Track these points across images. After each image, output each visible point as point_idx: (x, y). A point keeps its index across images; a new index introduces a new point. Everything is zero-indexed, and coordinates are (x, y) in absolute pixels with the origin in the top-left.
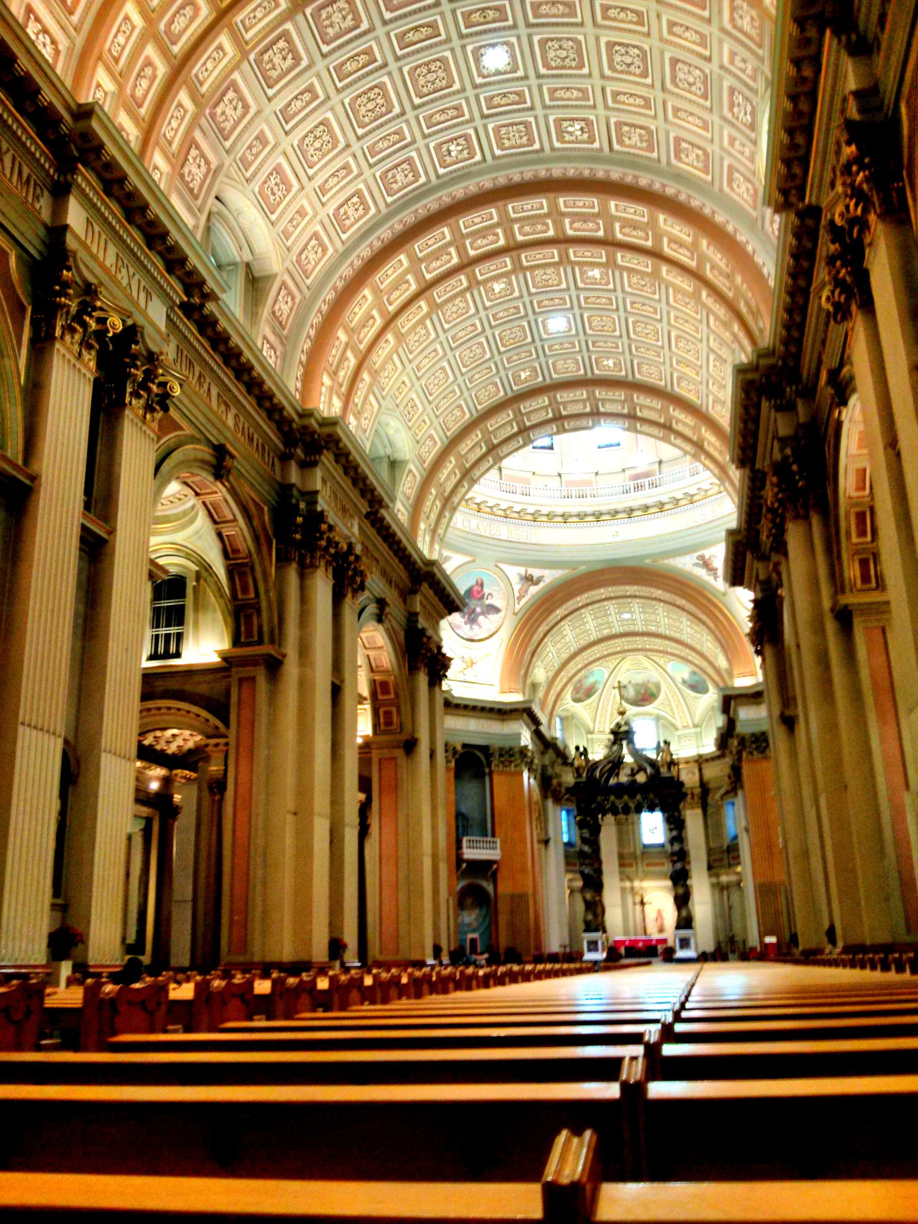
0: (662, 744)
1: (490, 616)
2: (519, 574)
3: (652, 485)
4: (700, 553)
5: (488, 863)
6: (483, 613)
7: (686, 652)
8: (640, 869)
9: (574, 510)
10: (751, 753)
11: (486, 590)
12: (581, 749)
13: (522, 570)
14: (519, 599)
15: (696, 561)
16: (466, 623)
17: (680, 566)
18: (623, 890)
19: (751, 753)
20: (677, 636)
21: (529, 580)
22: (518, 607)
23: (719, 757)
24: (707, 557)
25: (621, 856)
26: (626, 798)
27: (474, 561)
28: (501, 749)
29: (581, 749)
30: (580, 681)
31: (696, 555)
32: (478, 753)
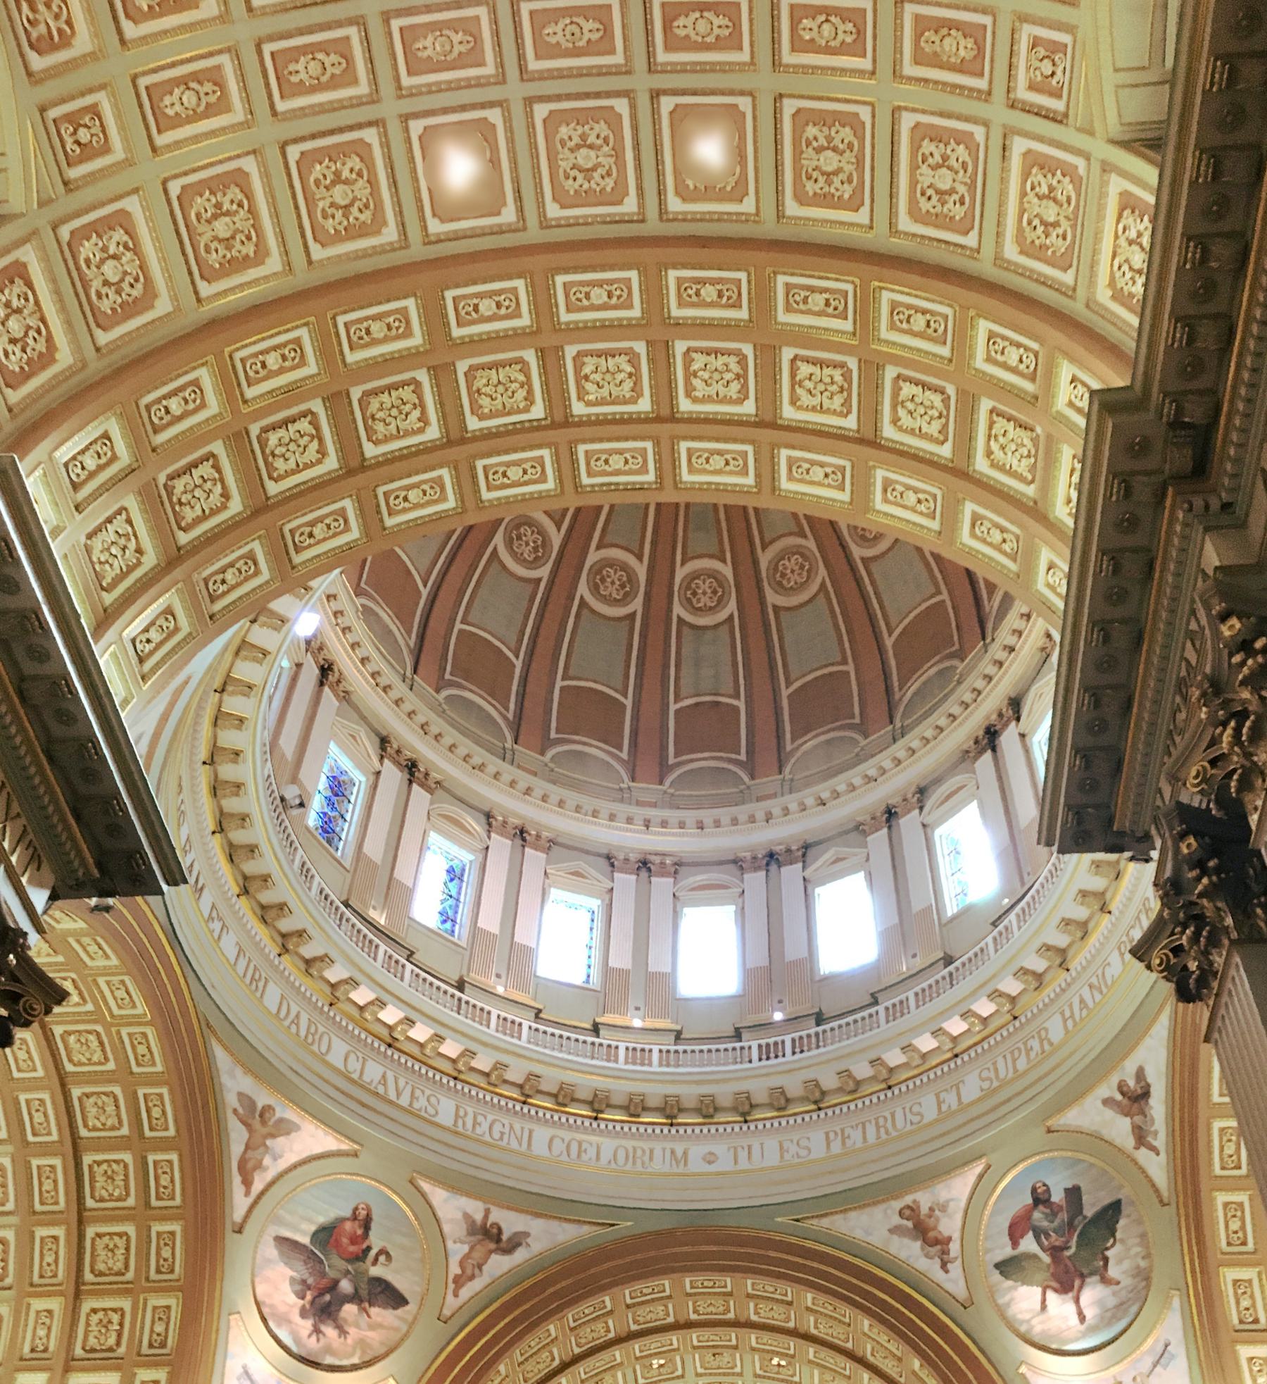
1: (374, 1311)
2: (466, 1216)
3: (799, 1046)
4: (908, 1200)
6: (355, 1298)
9: (621, 1089)
11: (376, 1240)
13: (476, 1209)
14: (459, 1282)
15: (896, 1220)
16: (303, 1313)
17: (859, 1234)
22: (452, 1303)
24: (924, 1210)
27: (356, 1155)
31: (897, 1205)
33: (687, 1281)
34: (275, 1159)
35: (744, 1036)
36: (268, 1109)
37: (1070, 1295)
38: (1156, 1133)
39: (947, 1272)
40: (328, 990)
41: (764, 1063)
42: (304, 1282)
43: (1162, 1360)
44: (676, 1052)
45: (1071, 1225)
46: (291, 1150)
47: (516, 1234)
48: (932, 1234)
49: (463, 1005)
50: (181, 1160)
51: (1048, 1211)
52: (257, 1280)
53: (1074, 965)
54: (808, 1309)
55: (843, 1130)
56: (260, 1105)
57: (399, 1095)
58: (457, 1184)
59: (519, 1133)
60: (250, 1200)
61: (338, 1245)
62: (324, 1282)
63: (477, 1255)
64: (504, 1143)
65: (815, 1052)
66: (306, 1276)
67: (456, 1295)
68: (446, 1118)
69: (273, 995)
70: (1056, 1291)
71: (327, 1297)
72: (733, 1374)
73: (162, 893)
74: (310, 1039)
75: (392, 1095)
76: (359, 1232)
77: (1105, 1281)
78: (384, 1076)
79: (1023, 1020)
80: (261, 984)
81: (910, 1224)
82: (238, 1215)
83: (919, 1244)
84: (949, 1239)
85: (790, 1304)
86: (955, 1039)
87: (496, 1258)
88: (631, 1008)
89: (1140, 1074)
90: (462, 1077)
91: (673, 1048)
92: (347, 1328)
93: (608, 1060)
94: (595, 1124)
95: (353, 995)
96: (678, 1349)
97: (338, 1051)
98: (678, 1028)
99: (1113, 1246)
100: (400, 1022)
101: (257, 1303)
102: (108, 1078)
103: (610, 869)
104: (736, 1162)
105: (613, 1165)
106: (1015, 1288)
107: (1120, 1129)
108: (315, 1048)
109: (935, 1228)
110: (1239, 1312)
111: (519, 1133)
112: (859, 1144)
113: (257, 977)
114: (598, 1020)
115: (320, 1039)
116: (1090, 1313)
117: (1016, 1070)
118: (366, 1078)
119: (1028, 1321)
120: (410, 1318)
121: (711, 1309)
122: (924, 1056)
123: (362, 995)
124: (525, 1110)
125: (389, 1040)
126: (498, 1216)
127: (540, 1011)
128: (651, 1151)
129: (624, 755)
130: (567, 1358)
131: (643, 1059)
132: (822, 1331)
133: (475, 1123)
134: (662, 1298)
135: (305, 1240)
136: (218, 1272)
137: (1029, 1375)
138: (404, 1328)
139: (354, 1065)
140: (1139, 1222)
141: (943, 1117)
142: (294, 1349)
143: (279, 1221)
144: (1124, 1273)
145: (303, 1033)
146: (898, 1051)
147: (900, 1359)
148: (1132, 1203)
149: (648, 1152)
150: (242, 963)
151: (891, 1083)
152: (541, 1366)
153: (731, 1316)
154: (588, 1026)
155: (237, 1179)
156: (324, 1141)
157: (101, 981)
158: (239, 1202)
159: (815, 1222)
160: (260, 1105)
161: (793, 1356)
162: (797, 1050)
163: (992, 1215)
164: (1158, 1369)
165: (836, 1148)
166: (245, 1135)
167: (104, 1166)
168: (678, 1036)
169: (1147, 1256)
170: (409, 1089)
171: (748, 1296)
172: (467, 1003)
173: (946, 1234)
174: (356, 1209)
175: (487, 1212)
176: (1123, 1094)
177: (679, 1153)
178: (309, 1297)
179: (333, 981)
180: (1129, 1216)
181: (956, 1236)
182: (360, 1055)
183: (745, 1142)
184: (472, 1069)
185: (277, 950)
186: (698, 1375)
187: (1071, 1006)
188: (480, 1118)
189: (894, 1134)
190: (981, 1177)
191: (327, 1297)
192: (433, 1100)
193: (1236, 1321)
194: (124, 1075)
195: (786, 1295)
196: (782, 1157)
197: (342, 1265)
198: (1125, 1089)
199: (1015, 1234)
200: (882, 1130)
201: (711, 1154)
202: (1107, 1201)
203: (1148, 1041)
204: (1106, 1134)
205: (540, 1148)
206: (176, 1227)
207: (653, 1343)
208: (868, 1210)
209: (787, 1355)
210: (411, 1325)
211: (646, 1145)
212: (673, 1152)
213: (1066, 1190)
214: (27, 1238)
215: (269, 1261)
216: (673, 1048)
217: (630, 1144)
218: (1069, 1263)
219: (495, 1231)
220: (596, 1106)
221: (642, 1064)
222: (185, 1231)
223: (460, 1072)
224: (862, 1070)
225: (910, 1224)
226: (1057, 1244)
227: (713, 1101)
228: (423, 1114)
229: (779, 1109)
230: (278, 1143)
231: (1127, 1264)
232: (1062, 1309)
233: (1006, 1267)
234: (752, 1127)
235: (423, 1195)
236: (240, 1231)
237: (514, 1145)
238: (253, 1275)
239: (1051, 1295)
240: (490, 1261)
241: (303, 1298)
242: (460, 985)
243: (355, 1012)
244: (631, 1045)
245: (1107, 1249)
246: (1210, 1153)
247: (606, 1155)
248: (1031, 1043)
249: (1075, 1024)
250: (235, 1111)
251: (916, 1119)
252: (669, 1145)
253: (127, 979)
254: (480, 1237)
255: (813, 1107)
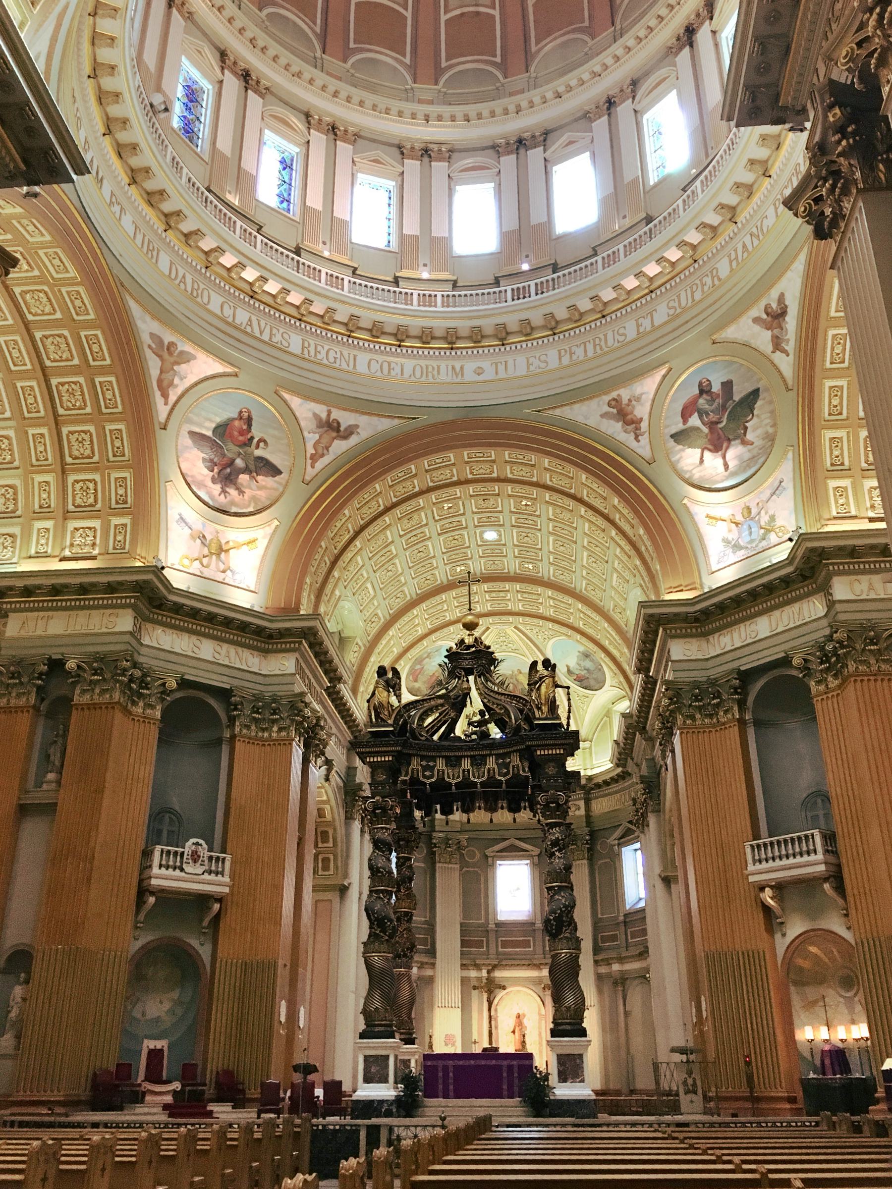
0: (540, 667)
1: (259, 478)
2: (315, 415)
4: (614, 394)
5: (203, 900)
6: (247, 470)
7: (577, 613)
8: (493, 950)
9: (415, 324)
10: (693, 718)
11: (256, 432)
12: (390, 675)
13: (321, 410)
14: (314, 458)
15: (606, 409)
16: (214, 480)
17: (580, 419)
18: (464, 981)
19: (693, 718)
20: (564, 579)
21: (331, 427)
22: (310, 472)
23: (614, 780)
24: (625, 401)
25: (465, 930)
26: (466, 764)
27: (236, 375)
28: (257, 698)
29: (390, 675)
30: (419, 661)
31: (607, 398)
32: (212, 702)
33: (465, 453)
34: (182, 379)
35: (502, 283)
36: (171, 345)
37: (720, 453)
38: (788, 340)
39: (638, 441)
40: (203, 256)
41: (516, 302)
42: (211, 460)
43: (777, 492)
44: (454, 296)
45: (724, 407)
46: (192, 373)
47: (350, 426)
48: (629, 417)
49: (301, 266)
50: (117, 381)
51: (709, 398)
52: (180, 460)
53: (741, 219)
54: (546, 469)
55: (570, 348)
56: (166, 343)
57: (261, 334)
58: (308, 394)
59: (347, 357)
60: (169, 407)
61: (231, 436)
62: (225, 460)
63: (325, 441)
64: (337, 365)
65: (551, 293)
66: (213, 457)
67: (313, 467)
68: (296, 348)
69: (164, 261)
70: (710, 450)
71: (228, 470)
72: (497, 512)
73: (72, 181)
74: (195, 294)
75: (258, 335)
76: (245, 427)
77: (744, 443)
78: (250, 320)
79: (701, 263)
80: (155, 253)
81: (615, 411)
82: (162, 417)
83: (620, 423)
84: (641, 419)
85: (534, 466)
86: (651, 280)
87: (336, 442)
88: (421, 264)
89: (781, 299)
90: (304, 319)
91: (451, 293)
92: (243, 489)
93: (406, 304)
94: (399, 350)
95: (222, 260)
96: (460, 498)
97: (215, 302)
98: (455, 278)
99: (751, 419)
100: (257, 280)
101: (182, 474)
102: (56, 324)
103: (401, 156)
104: (497, 373)
105: (413, 378)
106: (683, 450)
107: (763, 339)
108: (199, 299)
109: (632, 413)
110: (832, 459)
111: (347, 357)
112: (581, 358)
113: (151, 248)
114: (397, 274)
115: (202, 292)
116: (732, 464)
117: (693, 300)
118: (238, 321)
119: (691, 471)
120: (284, 482)
121: (481, 471)
122: (629, 293)
123: (228, 260)
124: (350, 341)
125: (251, 294)
126: (336, 414)
127: (355, 269)
128: (439, 367)
129: (407, 60)
130: (388, 505)
131: (430, 302)
132: (556, 482)
133: (316, 352)
134: (449, 465)
135: (209, 433)
136: (154, 457)
137: (689, 504)
138: (281, 489)
139: (228, 312)
140: (771, 402)
141: (640, 335)
142: (211, 503)
143: (190, 421)
144: (758, 437)
145: (189, 289)
146: (610, 289)
147: (605, 499)
148: (767, 390)
149: (436, 367)
150: (139, 237)
151: (605, 314)
152: (371, 510)
153: (495, 475)
154: (390, 279)
155: (158, 394)
156: (213, 366)
157: (41, 252)
158: (162, 411)
159: (550, 412)
160: (166, 343)
161: (535, 499)
162: (539, 292)
163: (671, 401)
164: (774, 497)
165: (566, 360)
166: (159, 363)
167: (66, 386)
168: (455, 285)
169: (774, 425)
170: (268, 327)
171: (506, 462)
172: (303, 264)
173: (639, 416)
174: (241, 412)
175: (329, 413)
176: (768, 314)
177: (458, 369)
178: (216, 470)
179: (206, 249)
180: (764, 399)
181: (646, 418)
182: (232, 304)
183: (502, 359)
184: (311, 313)
185: (163, 227)
186: (474, 513)
187: (736, 250)
188: (319, 348)
189: (606, 349)
190: (664, 377)
191: (228, 470)
192: (285, 335)
193: (829, 464)
194: (69, 322)
195: (531, 460)
196: (528, 368)
197: (237, 449)
198: (770, 310)
199: (685, 415)
200: (598, 347)
201: (479, 368)
202: (750, 390)
203: (789, 274)
204: (754, 343)
205: (362, 368)
206: (121, 426)
207: (444, 494)
208: (587, 403)
209: (531, 499)
210: (286, 486)
211: (434, 363)
212: (453, 368)
213: (722, 383)
214: (23, 435)
215: (187, 447)
216: (451, 293)
217: (423, 363)
218: (720, 431)
219: (335, 424)
220: (399, 337)
221: (430, 306)
222: (128, 428)
223: (303, 315)
224: (585, 305)
225: (615, 411)
226: (714, 419)
227: (480, 331)
228: (279, 345)
229: (527, 335)
230: (182, 368)
231: (759, 431)
232: (713, 461)
233: (677, 437)
234: (508, 348)
235: (285, 402)
236: (165, 429)
237: (344, 366)
238: (178, 457)
239: (707, 454)
240: (333, 444)
241: (212, 471)
242: (298, 251)
243: (224, 273)
244: (422, 293)
245: (747, 422)
246: (824, 352)
247: (408, 372)
248: (705, 279)
249: (738, 263)
250: (149, 346)
251: (621, 338)
252: (450, 363)
253: (58, 250)
254: (326, 429)
255: (551, 333)
